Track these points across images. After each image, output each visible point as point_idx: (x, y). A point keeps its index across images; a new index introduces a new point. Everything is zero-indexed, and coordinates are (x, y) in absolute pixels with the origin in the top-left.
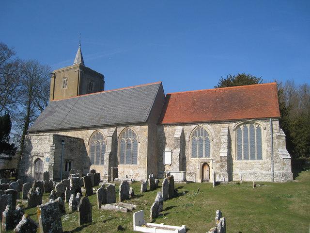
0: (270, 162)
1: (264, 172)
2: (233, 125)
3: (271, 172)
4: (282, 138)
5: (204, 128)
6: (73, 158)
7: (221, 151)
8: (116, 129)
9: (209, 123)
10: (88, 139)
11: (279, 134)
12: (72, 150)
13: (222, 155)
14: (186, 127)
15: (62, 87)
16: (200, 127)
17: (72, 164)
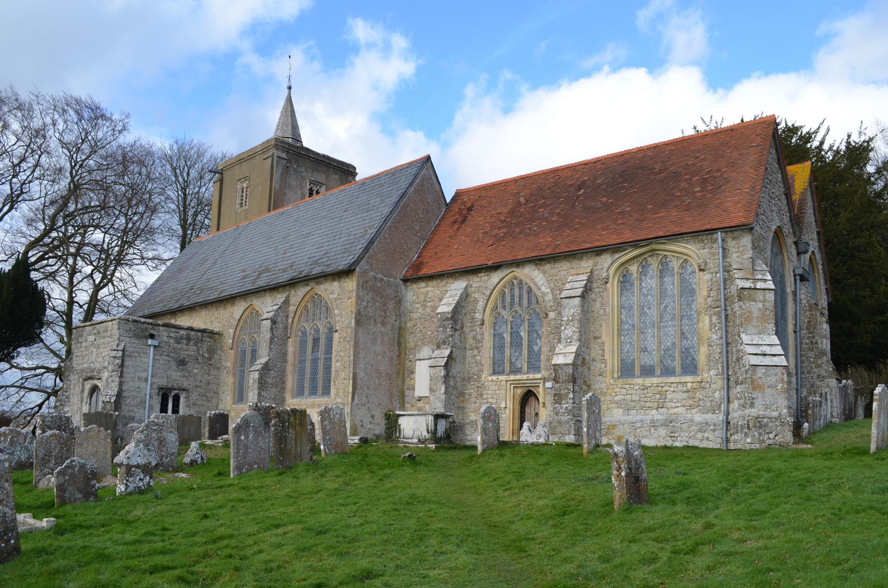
0: (719, 383)
1: (698, 418)
2: (606, 263)
3: (721, 417)
4: (760, 295)
5: (525, 280)
6: (186, 385)
7: (560, 348)
8: (288, 297)
9: (539, 261)
10: (231, 331)
11: (748, 284)
12: (182, 363)
13: (558, 360)
14: (476, 281)
15: (237, 206)
16: (516, 278)
17: (182, 400)
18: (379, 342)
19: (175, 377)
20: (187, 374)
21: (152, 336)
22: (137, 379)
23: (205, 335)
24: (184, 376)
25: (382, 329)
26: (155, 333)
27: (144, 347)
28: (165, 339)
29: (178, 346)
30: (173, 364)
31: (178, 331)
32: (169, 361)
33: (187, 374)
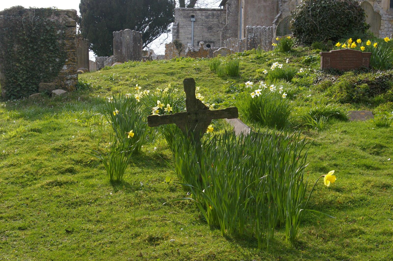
6: (213, 39)
18: (262, 11)
19: (208, 36)
20: (213, 34)
21: (193, 16)
22: (186, 38)
23: (223, 12)
24: (211, 35)
25: (265, 4)
26: (194, 15)
27: (189, 22)
28: (200, 17)
29: (208, 20)
30: (205, 30)
31: (207, 12)
32: (203, 28)
33: (213, 34)
